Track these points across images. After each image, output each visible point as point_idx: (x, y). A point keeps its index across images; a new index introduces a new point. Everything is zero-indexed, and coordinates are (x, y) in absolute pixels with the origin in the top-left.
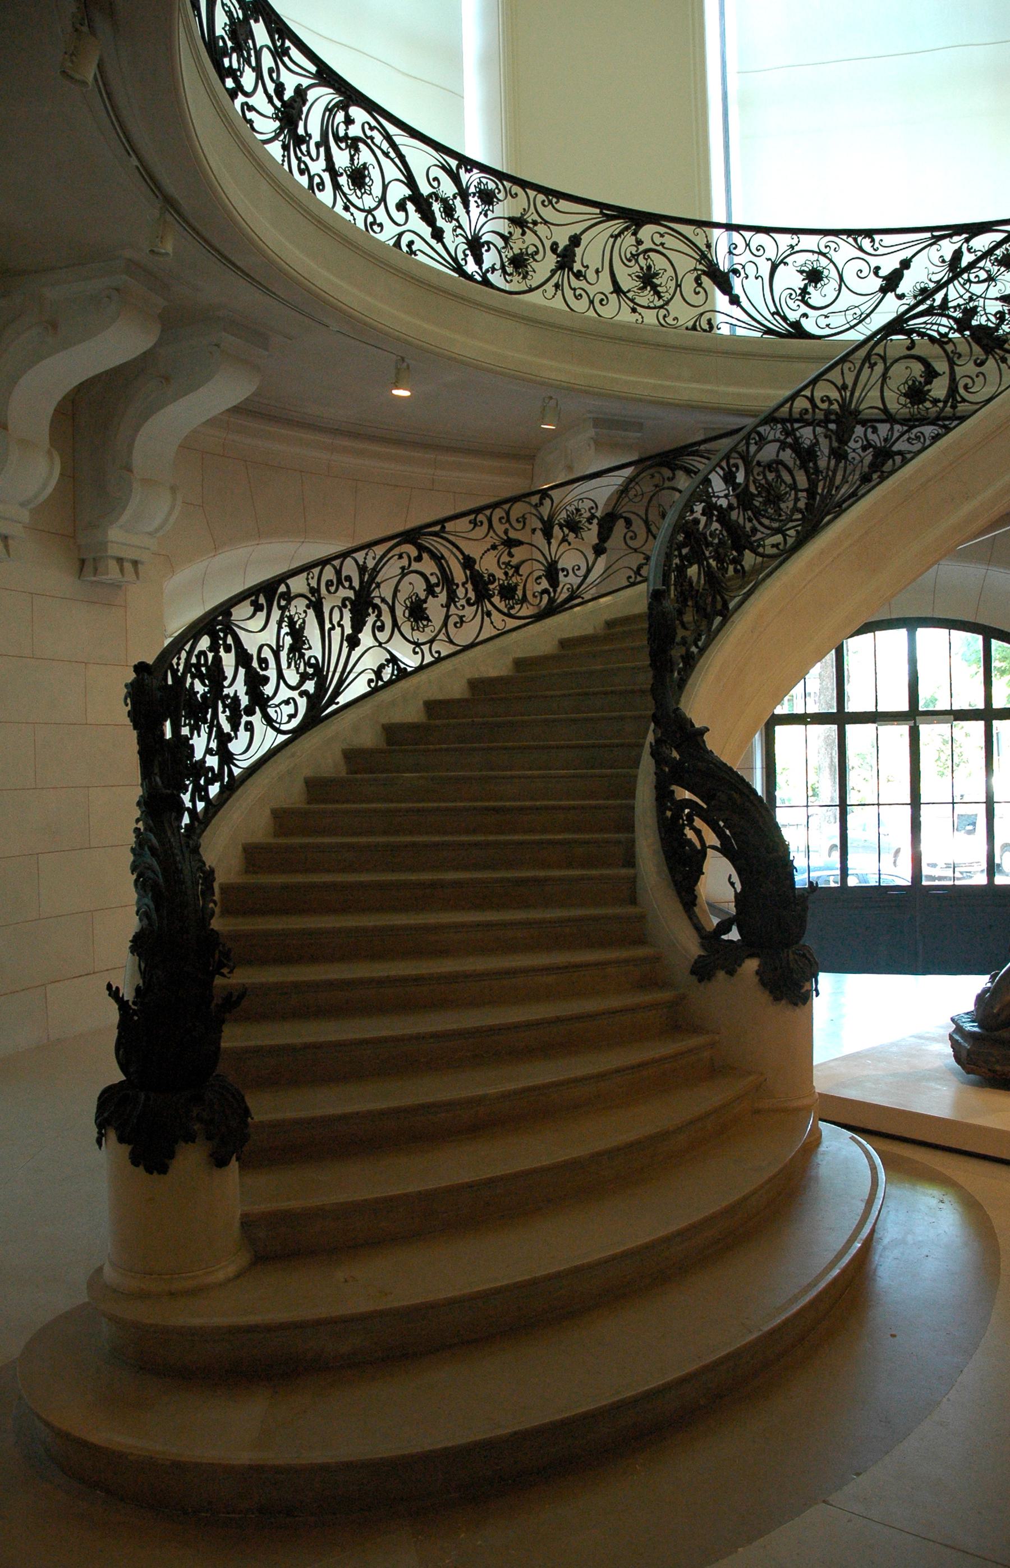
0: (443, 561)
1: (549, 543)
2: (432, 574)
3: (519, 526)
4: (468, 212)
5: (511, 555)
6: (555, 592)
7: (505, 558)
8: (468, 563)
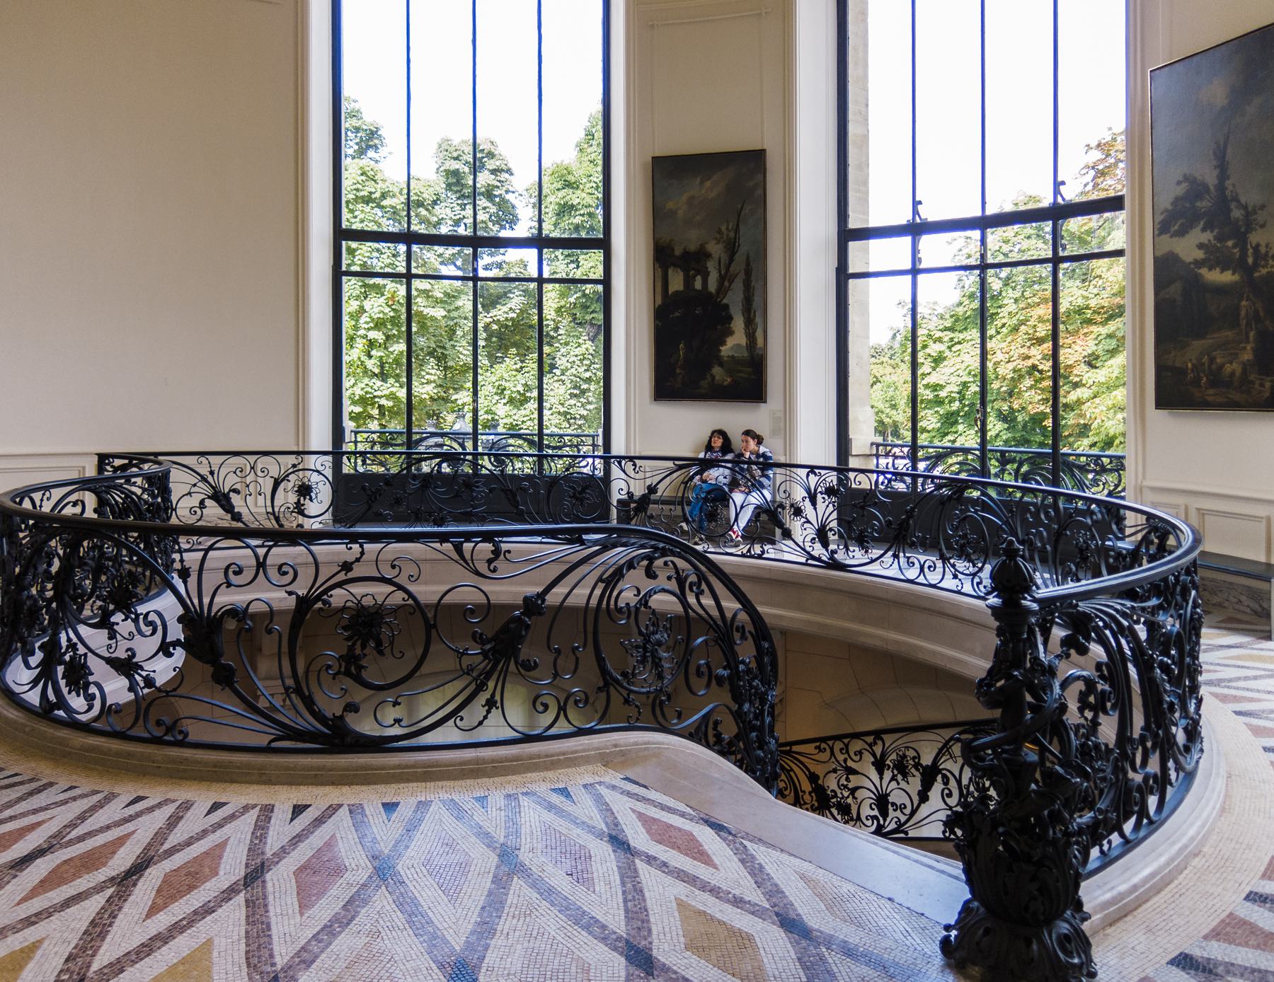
0: (792, 773)
1: (881, 779)
3: (857, 758)
5: (848, 779)
6: (885, 820)
7: (843, 781)
8: (813, 778)
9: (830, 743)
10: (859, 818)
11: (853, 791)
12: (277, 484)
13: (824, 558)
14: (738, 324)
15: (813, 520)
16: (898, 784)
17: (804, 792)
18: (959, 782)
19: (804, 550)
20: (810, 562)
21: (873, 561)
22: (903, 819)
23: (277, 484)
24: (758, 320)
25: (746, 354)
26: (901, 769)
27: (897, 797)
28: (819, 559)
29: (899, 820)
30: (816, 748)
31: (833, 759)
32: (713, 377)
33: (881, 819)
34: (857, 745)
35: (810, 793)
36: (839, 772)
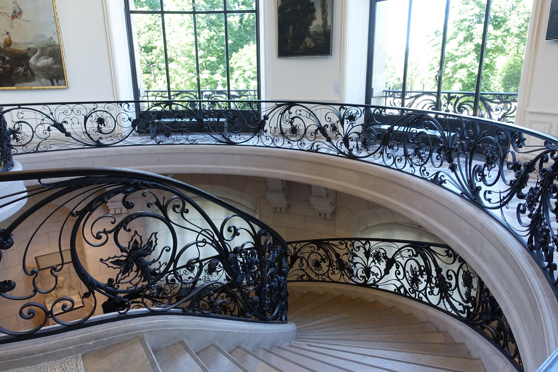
0: (328, 252)
1: (368, 260)
2: (323, 255)
3: (357, 250)
4: (343, 127)
5: (353, 258)
6: (368, 279)
7: (350, 259)
9: (346, 241)
10: (357, 275)
11: (355, 264)
12: (86, 118)
13: (347, 153)
14: (318, 13)
15: (342, 132)
16: (375, 264)
17: (334, 261)
18: (404, 269)
19: (337, 148)
20: (340, 154)
21: (370, 155)
22: (377, 280)
23: (86, 118)
24: (329, 10)
25: (322, 30)
26: (377, 257)
27: (374, 269)
28: (344, 153)
29: (375, 280)
30: (339, 243)
31: (346, 248)
32: (306, 43)
33: (367, 278)
34: (357, 244)
35: (336, 262)
36: (349, 255)
